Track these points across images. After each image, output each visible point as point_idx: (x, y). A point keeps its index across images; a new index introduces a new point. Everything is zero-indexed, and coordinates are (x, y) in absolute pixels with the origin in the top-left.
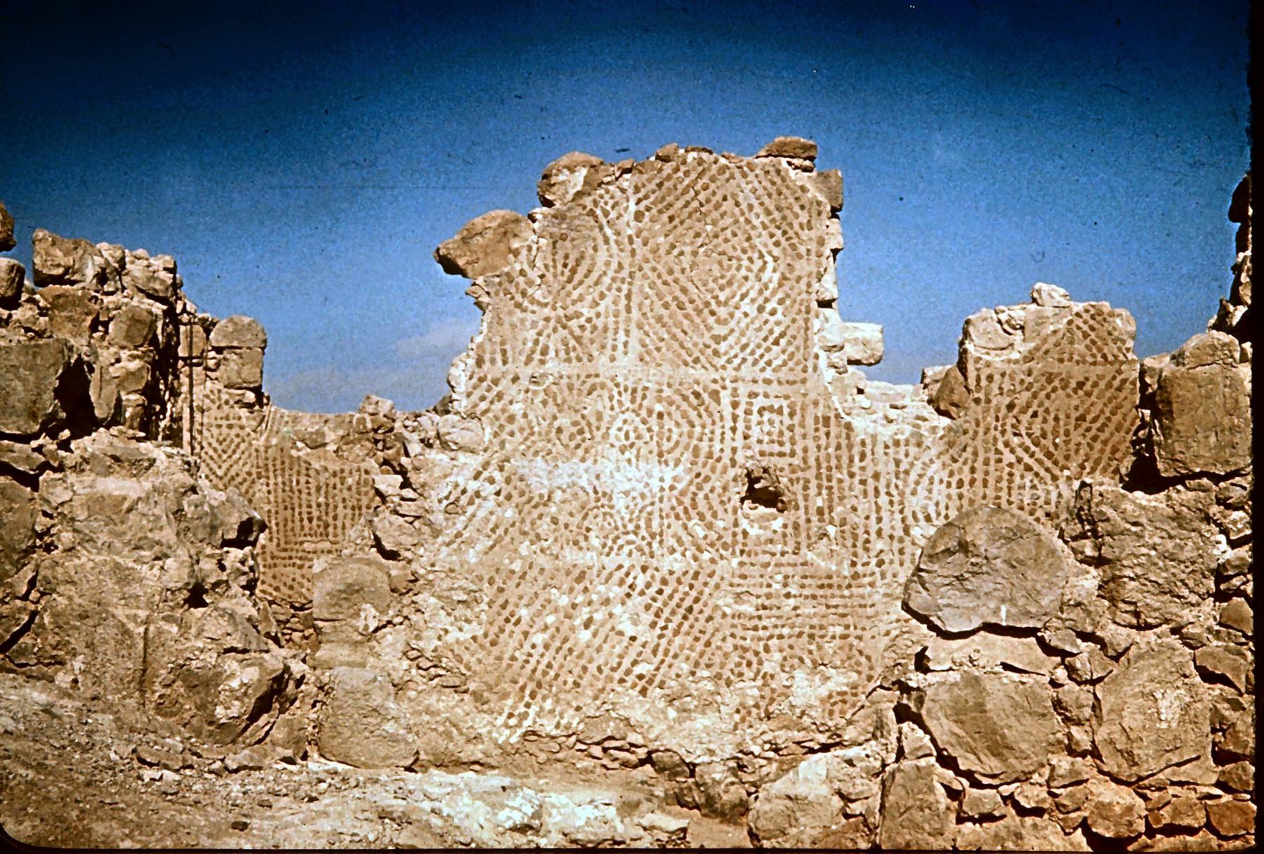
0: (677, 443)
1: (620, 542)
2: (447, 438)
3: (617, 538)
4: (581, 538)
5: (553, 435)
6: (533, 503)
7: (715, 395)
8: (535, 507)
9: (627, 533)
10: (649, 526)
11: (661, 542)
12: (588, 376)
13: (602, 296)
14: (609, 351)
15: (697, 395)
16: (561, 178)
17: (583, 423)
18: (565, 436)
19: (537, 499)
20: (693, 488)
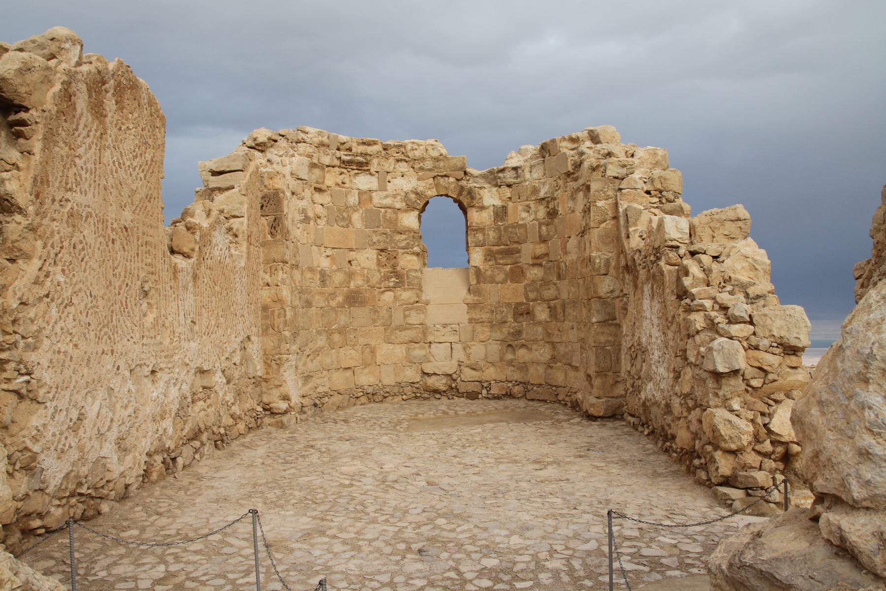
0: (120, 262)
1: (102, 333)
2: (16, 244)
3: (101, 330)
4: (86, 331)
5: (72, 250)
6: (64, 305)
7: (132, 229)
8: (65, 307)
9: (104, 327)
10: (112, 322)
11: (117, 333)
12: (85, 206)
13: (90, 148)
14: (92, 188)
15: (125, 228)
16: (67, 46)
17: (84, 241)
18: (77, 251)
19: (66, 302)
20: (126, 295)
